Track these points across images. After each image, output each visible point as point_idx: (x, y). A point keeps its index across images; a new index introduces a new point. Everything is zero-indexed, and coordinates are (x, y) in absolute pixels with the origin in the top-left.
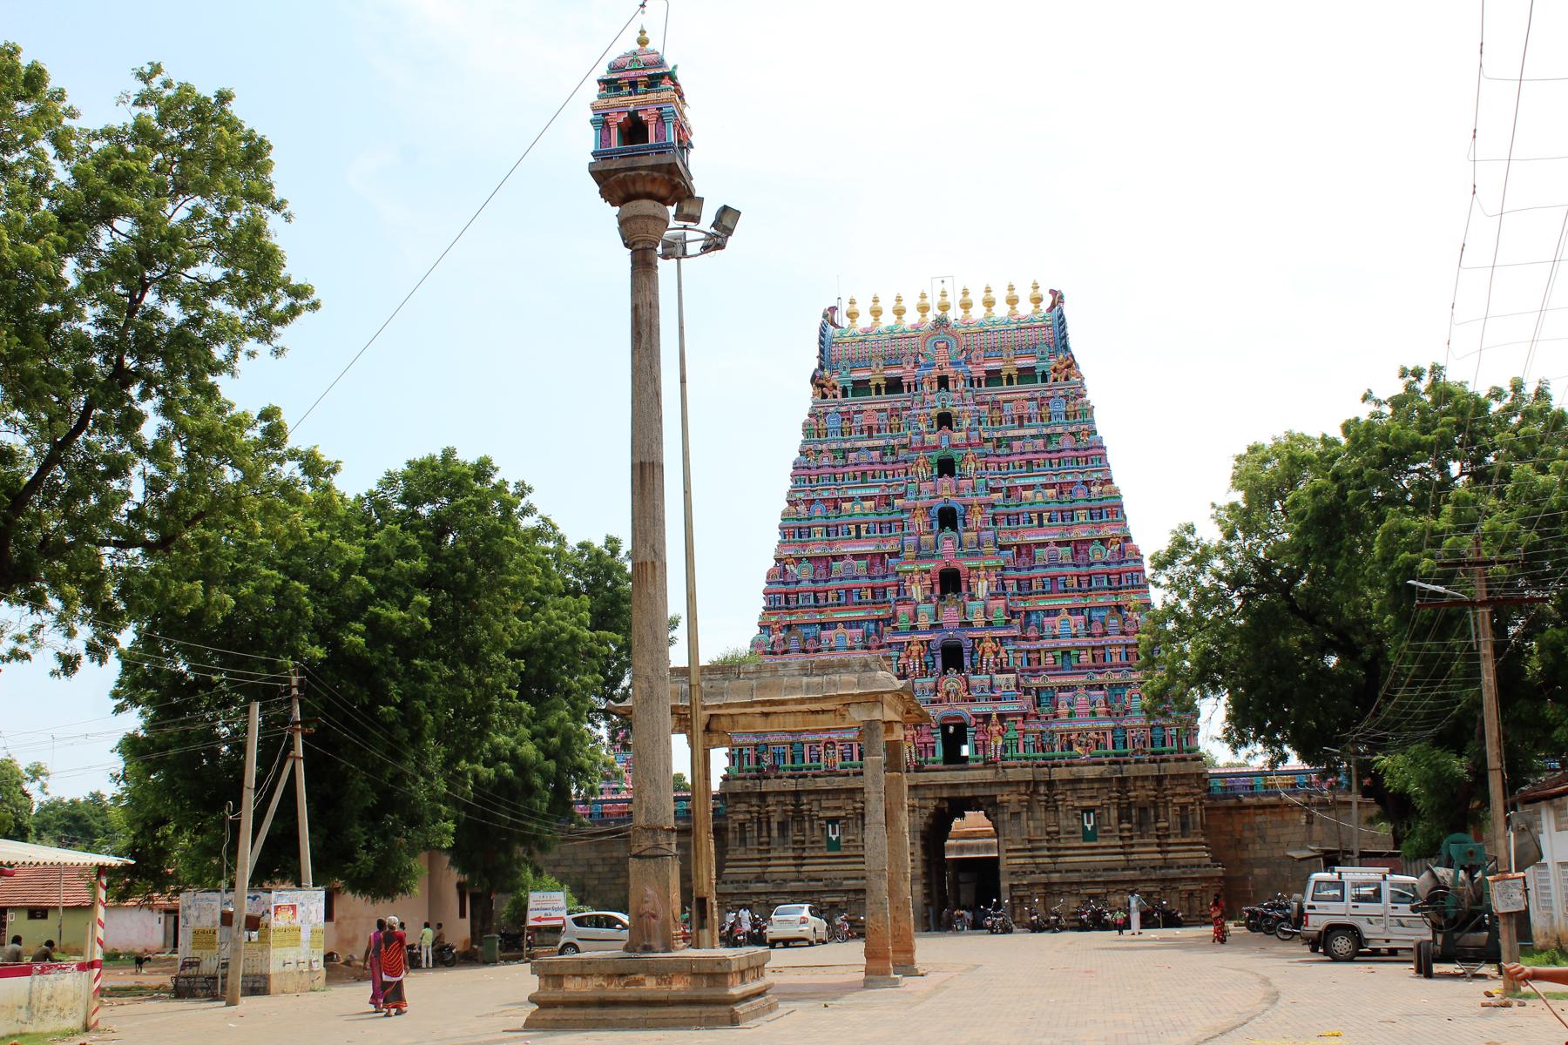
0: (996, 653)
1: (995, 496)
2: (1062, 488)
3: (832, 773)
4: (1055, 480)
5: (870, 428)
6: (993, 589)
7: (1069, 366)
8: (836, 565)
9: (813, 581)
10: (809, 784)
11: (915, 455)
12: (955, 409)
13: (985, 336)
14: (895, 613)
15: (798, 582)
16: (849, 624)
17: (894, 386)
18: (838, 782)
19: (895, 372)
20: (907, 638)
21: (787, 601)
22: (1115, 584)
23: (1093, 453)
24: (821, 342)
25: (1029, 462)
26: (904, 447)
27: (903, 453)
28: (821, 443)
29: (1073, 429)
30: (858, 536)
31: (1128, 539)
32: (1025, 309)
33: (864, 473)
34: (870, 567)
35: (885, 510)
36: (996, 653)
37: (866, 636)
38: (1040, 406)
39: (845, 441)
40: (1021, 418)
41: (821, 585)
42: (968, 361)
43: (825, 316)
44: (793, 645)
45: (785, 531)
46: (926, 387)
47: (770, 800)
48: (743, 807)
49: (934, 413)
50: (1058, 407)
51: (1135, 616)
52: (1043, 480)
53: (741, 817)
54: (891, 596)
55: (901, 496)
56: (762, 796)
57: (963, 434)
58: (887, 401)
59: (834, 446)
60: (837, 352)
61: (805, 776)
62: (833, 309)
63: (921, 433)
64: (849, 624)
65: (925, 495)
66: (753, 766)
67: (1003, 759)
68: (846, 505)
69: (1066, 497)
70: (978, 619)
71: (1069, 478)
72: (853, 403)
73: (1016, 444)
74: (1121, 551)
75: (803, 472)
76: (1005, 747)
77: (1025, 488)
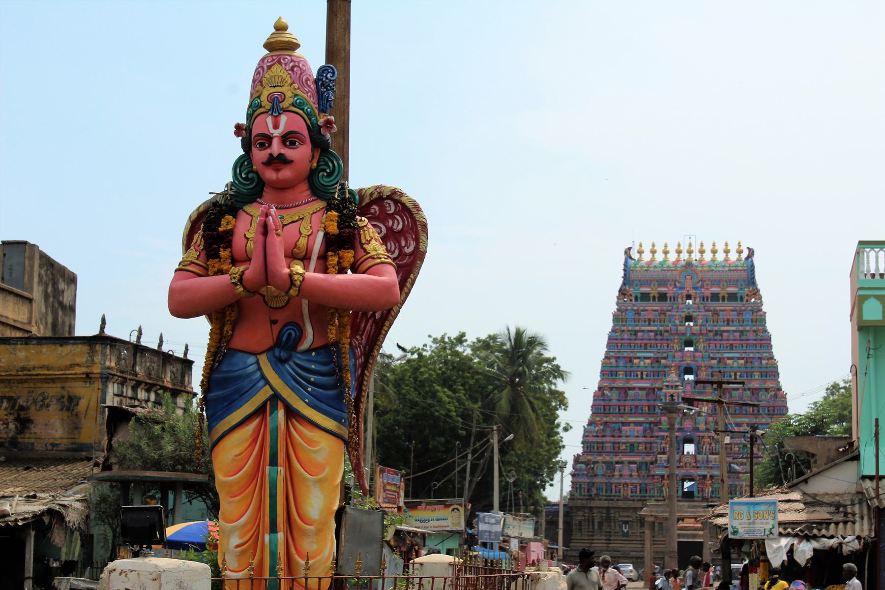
0: (710, 444)
1: (715, 362)
2: (748, 360)
3: (626, 499)
4: (744, 355)
5: (649, 320)
6: (710, 411)
7: (755, 294)
8: (631, 393)
9: (618, 400)
10: (614, 504)
11: (672, 337)
12: (695, 314)
13: (711, 273)
14: (660, 421)
15: (610, 400)
17: (663, 297)
18: (629, 504)
19: (663, 289)
21: (604, 409)
22: (771, 412)
23: (765, 342)
24: (625, 270)
25: (731, 345)
26: (667, 331)
27: (666, 334)
28: (624, 326)
29: (755, 328)
30: (642, 378)
31: (779, 389)
32: (733, 256)
33: (646, 344)
34: (647, 395)
35: (656, 365)
36: (710, 444)
37: (645, 431)
38: (739, 315)
39: (636, 326)
40: (728, 320)
41: (622, 403)
42: (702, 286)
43: (626, 252)
44: (608, 433)
45: (603, 373)
46: (680, 300)
47: (595, 511)
48: (581, 513)
49: (683, 315)
50: (748, 316)
53: (580, 518)
55: (665, 358)
56: (591, 508)
57: (698, 328)
58: (657, 306)
59: (630, 328)
60: (633, 276)
61: (612, 500)
62: (630, 249)
63: (676, 325)
64: (637, 424)
65: (678, 359)
66: (586, 493)
67: (711, 497)
68: (636, 361)
69: (749, 365)
70: (702, 427)
71: (751, 355)
72: (640, 305)
73: (725, 334)
74: (776, 396)
75: (613, 342)
76: (712, 492)
77: (729, 358)
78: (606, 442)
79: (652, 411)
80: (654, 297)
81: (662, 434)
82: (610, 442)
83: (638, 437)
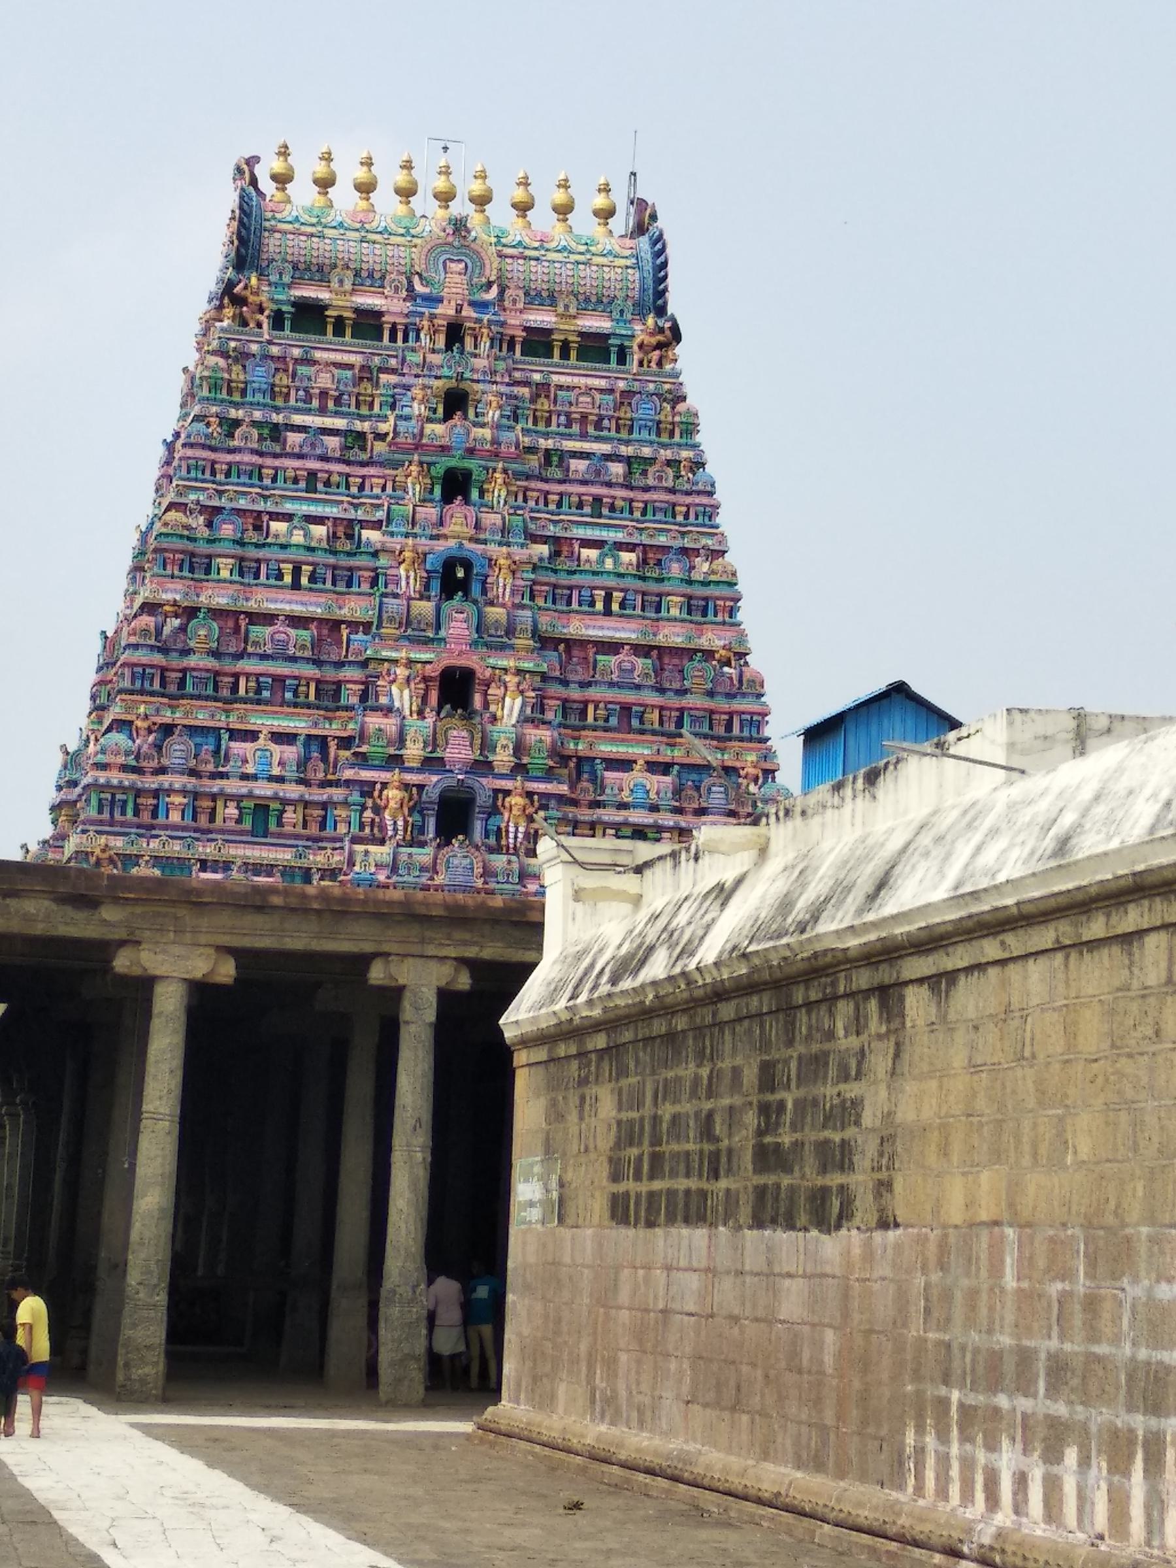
16: (281, 738)
20: (384, 776)
26: (381, 437)
30: (296, 585)
36: (530, 819)
46: (425, 339)
50: (644, 411)
51: (753, 788)
52: (620, 536)
54: (349, 696)
55: (377, 525)
57: (487, 433)
59: (258, 415)
64: (281, 738)
68: (278, 527)
72: (291, 343)
77: (587, 543)
78: (169, 792)
79: (573, 720)
80: (340, 320)
81: (366, 775)
82: (184, 792)
83: (280, 779)
